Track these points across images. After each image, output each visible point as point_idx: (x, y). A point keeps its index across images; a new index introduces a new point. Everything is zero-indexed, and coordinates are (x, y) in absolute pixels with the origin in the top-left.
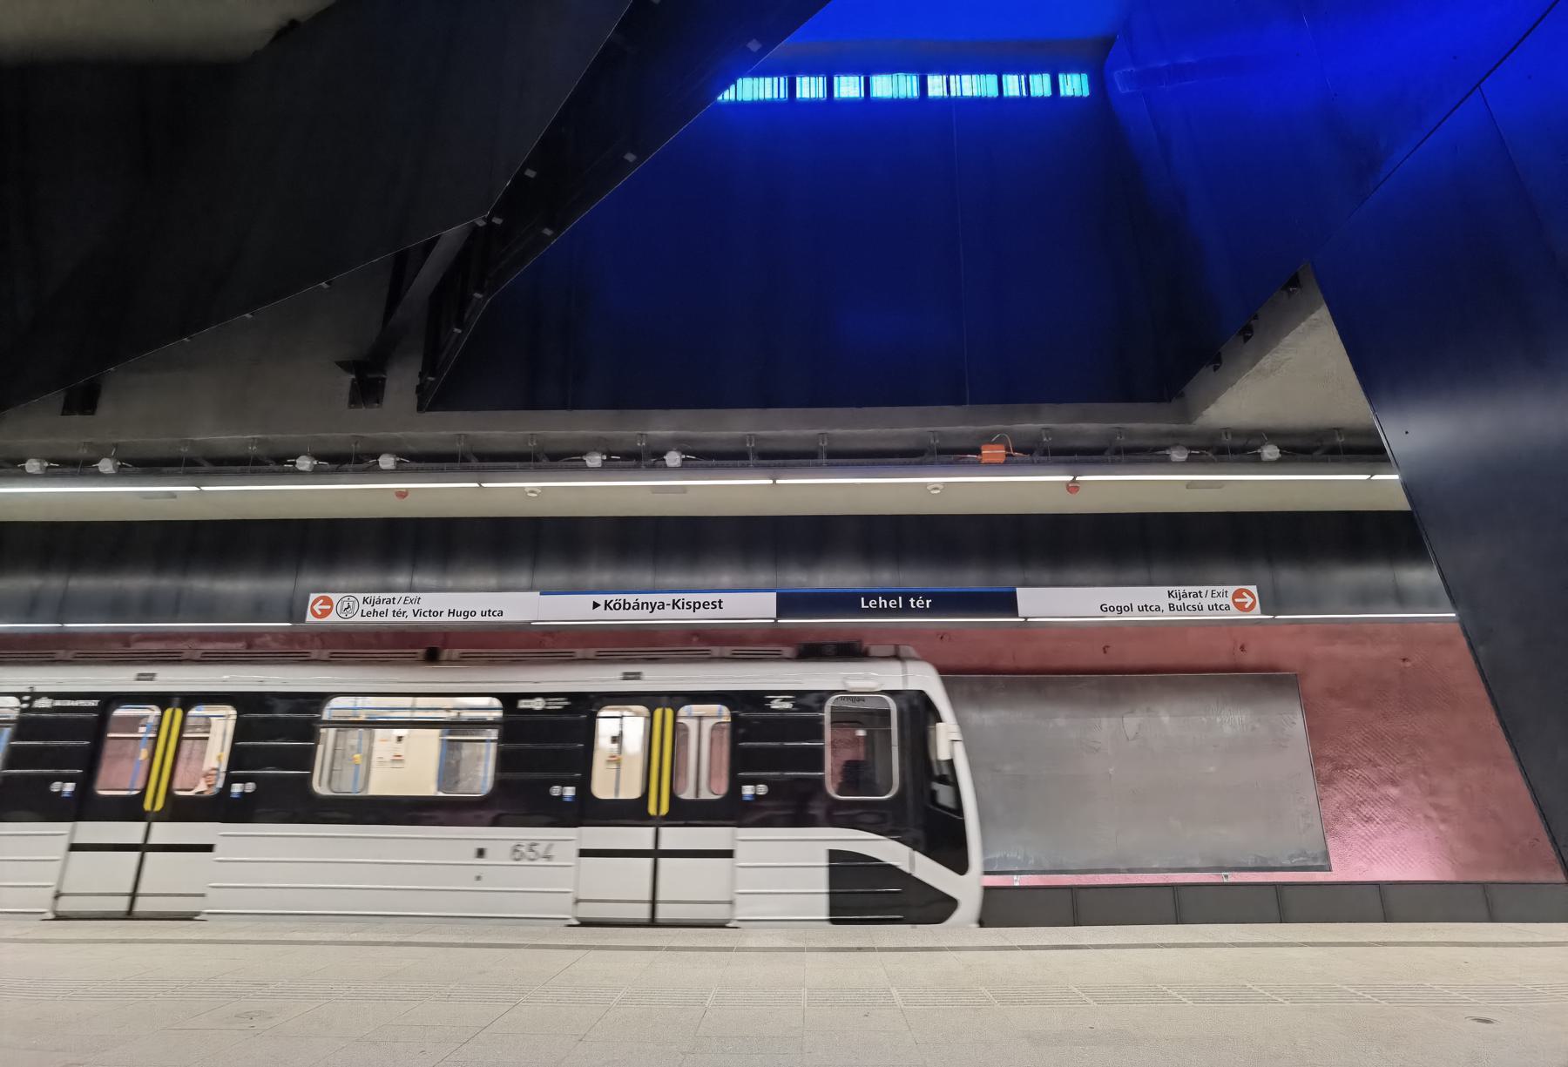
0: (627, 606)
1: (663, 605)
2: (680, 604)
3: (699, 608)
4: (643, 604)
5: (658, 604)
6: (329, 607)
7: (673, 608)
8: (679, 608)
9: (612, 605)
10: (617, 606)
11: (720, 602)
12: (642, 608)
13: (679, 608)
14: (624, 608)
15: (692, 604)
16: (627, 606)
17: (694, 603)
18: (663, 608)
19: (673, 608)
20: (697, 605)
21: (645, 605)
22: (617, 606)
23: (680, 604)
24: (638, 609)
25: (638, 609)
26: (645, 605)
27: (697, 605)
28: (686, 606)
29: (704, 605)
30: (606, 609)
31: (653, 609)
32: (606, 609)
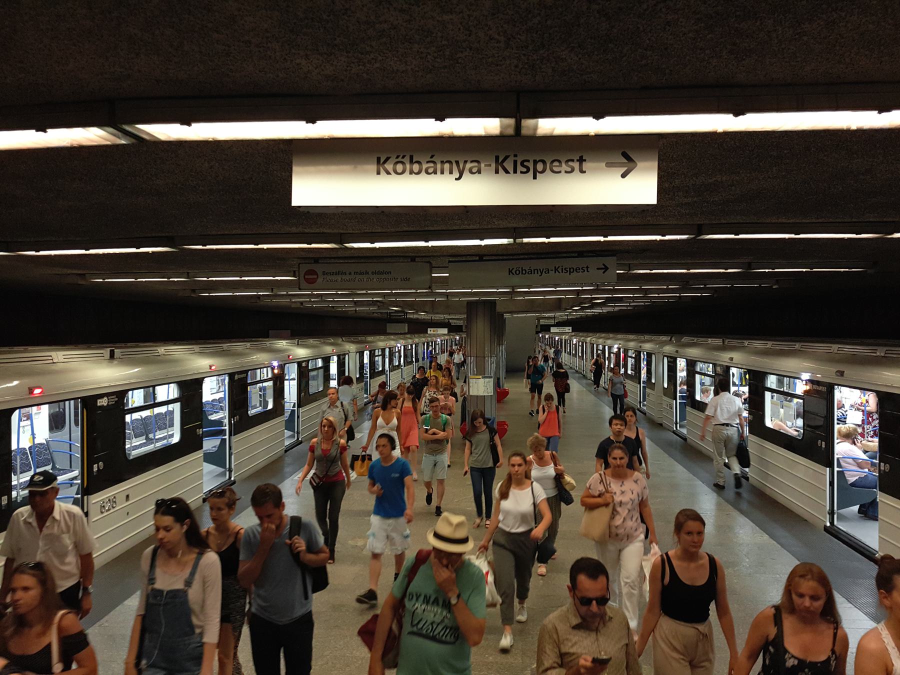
0: (524, 272)
1: (548, 271)
2: (560, 270)
3: (573, 272)
4: (534, 270)
5: (544, 270)
6: (306, 277)
7: (555, 272)
8: (559, 272)
9: (513, 271)
10: (518, 272)
11: (587, 267)
12: (534, 273)
13: (559, 272)
14: (522, 273)
15: (568, 269)
16: (524, 272)
17: (570, 269)
18: (548, 273)
19: (555, 272)
20: (572, 270)
21: (536, 271)
22: (518, 272)
23: (560, 270)
24: (531, 273)
25: (531, 273)
26: (536, 271)
27: (572, 270)
28: (564, 271)
29: (576, 270)
30: (509, 274)
31: (542, 273)
32: (509, 274)
